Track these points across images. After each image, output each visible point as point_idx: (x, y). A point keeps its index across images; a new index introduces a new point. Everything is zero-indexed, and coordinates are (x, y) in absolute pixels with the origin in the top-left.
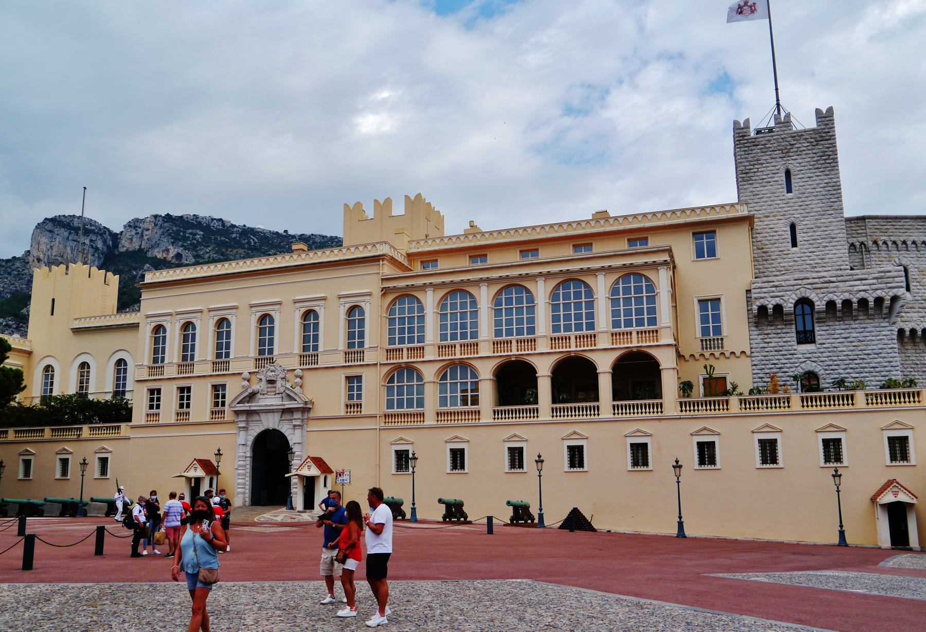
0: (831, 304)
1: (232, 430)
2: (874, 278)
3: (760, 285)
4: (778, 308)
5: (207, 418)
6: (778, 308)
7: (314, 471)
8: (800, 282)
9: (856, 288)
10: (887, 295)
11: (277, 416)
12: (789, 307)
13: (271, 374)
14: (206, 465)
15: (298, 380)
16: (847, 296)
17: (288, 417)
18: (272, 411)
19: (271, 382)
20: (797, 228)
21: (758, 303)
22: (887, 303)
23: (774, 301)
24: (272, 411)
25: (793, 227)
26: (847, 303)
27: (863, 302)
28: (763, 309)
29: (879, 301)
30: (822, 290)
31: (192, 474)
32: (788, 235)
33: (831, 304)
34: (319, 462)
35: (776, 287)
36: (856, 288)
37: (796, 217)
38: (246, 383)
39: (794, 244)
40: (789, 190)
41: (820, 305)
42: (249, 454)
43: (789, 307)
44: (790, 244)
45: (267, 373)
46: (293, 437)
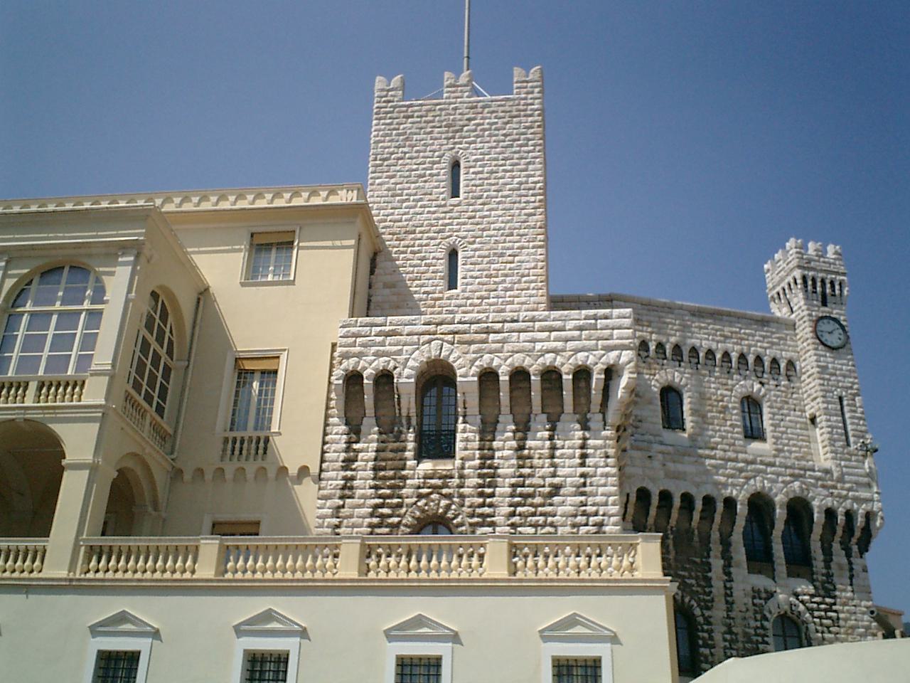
0: (488, 377)
2: (581, 329)
3: (353, 330)
4: (385, 379)
6: (385, 379)
8: (432, 328)
9: (538, 346)
10: (597, 362)
12: (406, 378)
16: (518, 360)
20: (460, 255)
21: (350, 364)
22: (597, 377)
23: (380, 363)
25: (453, 254)
26: (519, 375)
27: (551, 376)
28: (353, 379)
29: (582, 374)
30: (473, 347)
32: (442, 266)
33: (488, 377)
35: (387, 335)
36: (538, 346)
37: (460, 233)
39: (452, 284)
40: (455, 193)
41: (466, 375)
43: (406, 378)
44: (443, 284)
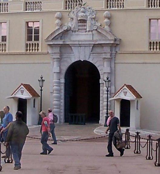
1: (48, 59)
5: (23, 51)
7: (130, 96)
11: (88, 50)
13: (81, 14)
14: (29, 88)
15: (106, 20)
17: (98, 50)
18: (85, 46)
19: (83, 21)
24: (85, 46)
31: (20, 96)
34: (130, 88)
38: (57, 21)
42: (63, 81)
45: (78, 13)
46: (103, 69)
